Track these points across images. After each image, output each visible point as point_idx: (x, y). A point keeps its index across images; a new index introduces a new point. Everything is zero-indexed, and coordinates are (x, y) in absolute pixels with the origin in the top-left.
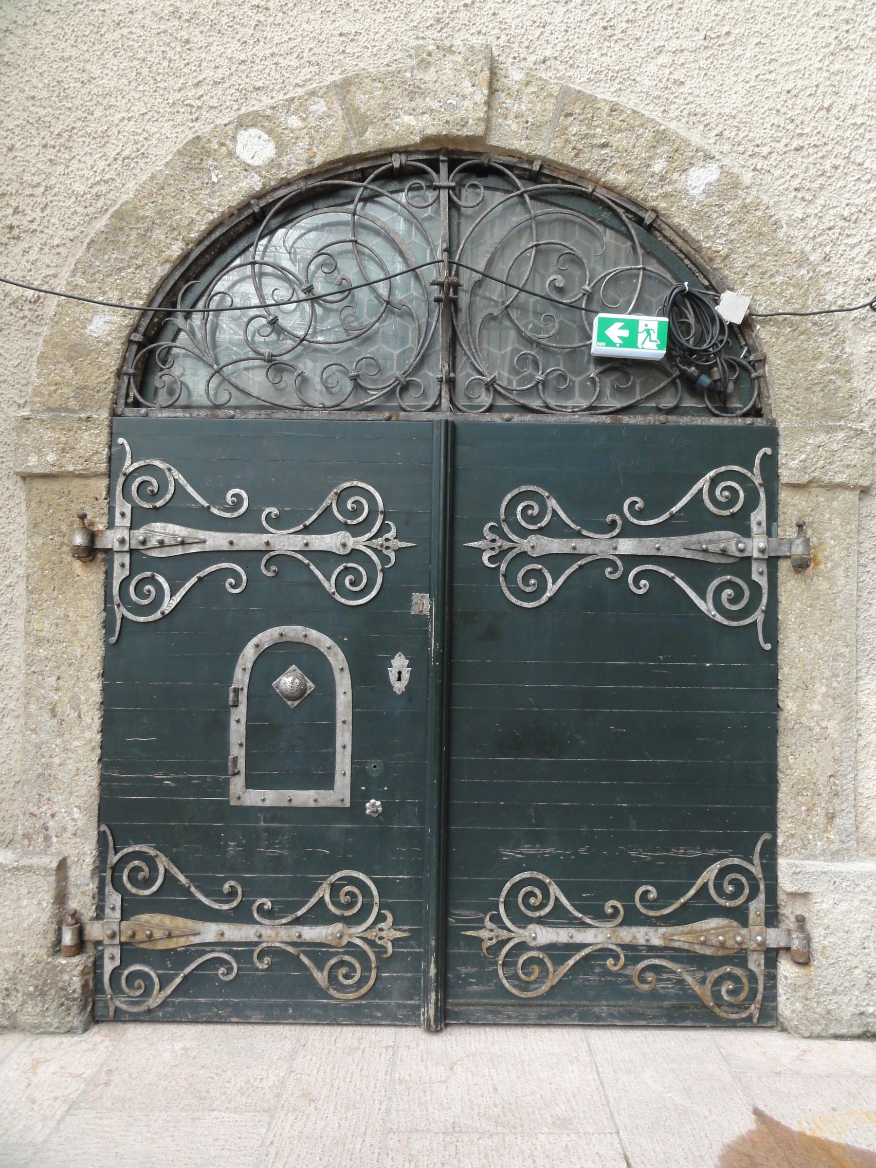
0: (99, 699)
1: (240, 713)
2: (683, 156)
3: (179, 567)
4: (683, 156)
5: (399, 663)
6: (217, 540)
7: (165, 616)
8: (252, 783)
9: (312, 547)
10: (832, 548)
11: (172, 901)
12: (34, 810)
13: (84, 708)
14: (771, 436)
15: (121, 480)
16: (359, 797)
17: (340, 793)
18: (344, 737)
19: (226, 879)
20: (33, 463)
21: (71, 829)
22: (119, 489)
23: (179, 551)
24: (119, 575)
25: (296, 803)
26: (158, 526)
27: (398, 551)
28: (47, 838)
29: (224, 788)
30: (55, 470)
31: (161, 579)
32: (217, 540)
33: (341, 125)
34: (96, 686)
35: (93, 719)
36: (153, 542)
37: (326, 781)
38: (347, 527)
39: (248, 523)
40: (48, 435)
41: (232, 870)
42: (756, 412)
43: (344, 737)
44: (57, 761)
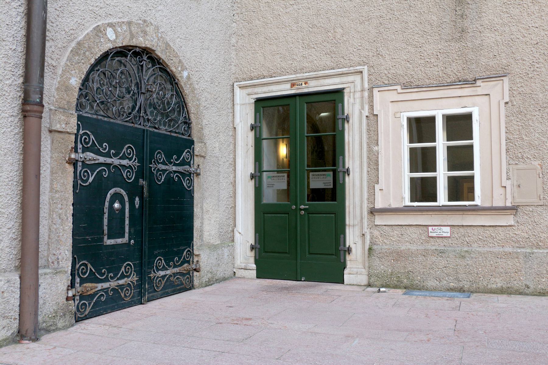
0: (72, 212)
1: (106, 216)
2: (184, 69)
3: (93, 167)
4: (184, 69)
5: (137, 199)
6: (102, 159)
7: (90, 184)
8: (108, 238)
9: (122, 164)
10: (202, 171)
11: (93, 279)
12: (55, 253)
13: (68, 215)
14: (192, 142)
15: (79, 136)
16: (130, 239)
17: (125, 240)
18: (127, 222)
19: (102, 269)
20: (58, 127)
21: (65, 258)
22: (79, 139)
23: (93, 162)
24: (79, 169)
25: (118, 243)
26: (88, 153)
27: (138, 166)
28: (58, 262)
29: (102, 240)
30: (64, 130)
31: (89, 171)
32: (102, 159)
33: (128, 37)
34: (72, 208)
35: (71, 219)
36: (88, 159)
37: (123, 236)
38: (128, 158)
39: (108, 155)
40: (63, 118)
41: (104, 266)
42: (189, 136)
43: (127, 222)
44: (61, 234)
